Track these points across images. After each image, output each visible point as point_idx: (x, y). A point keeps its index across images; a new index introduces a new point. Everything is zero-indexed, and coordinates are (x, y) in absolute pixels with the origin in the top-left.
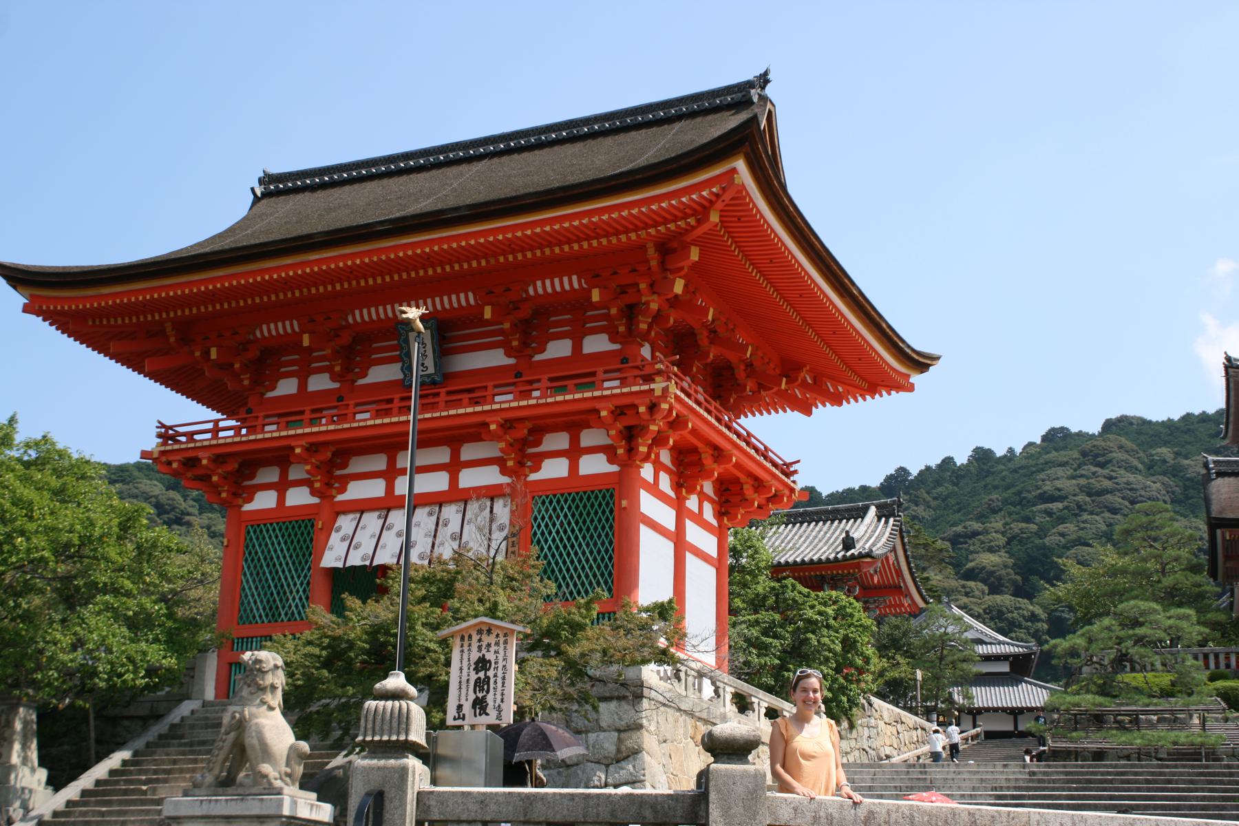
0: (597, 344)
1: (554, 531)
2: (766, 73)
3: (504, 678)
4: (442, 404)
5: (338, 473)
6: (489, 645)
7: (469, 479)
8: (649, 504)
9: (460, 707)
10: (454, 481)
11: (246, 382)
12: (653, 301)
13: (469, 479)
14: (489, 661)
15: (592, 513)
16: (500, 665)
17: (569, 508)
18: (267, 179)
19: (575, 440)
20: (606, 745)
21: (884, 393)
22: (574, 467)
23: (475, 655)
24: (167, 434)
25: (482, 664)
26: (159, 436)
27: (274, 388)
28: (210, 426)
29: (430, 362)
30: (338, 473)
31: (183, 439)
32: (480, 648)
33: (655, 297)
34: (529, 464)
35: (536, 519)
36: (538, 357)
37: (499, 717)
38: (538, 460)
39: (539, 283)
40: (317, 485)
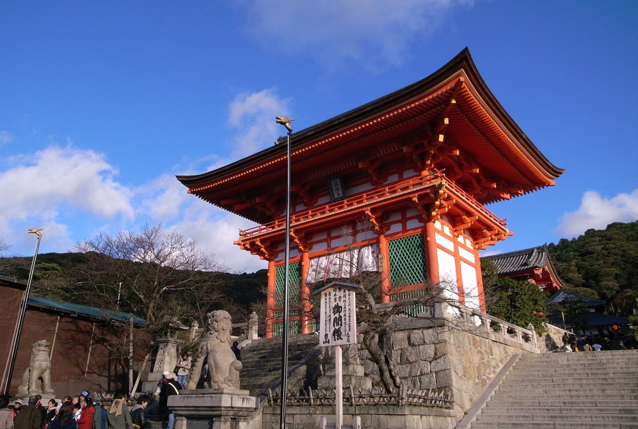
1: (399, 256)
3: (350, 316)
5: (309, 242)
6: (340, 297)
8: (439, 239)
9: (326, 335)
12: (431, 149)
14: (341, 307)
15: (413, 242)
16: (347, 309)
17: (404, 244)
19: (404, 215)
20: (429, 351)
21: (541, 188)
23: (333, 304)
24: (243, 234)
25: (337, 309)
26: (241, 235)
28: (258, 228)
29: (340, 192)
31: (249, 235)
33: (433, 148)
34: (385, 228)
35: (390, 251)
37: (348, 341)
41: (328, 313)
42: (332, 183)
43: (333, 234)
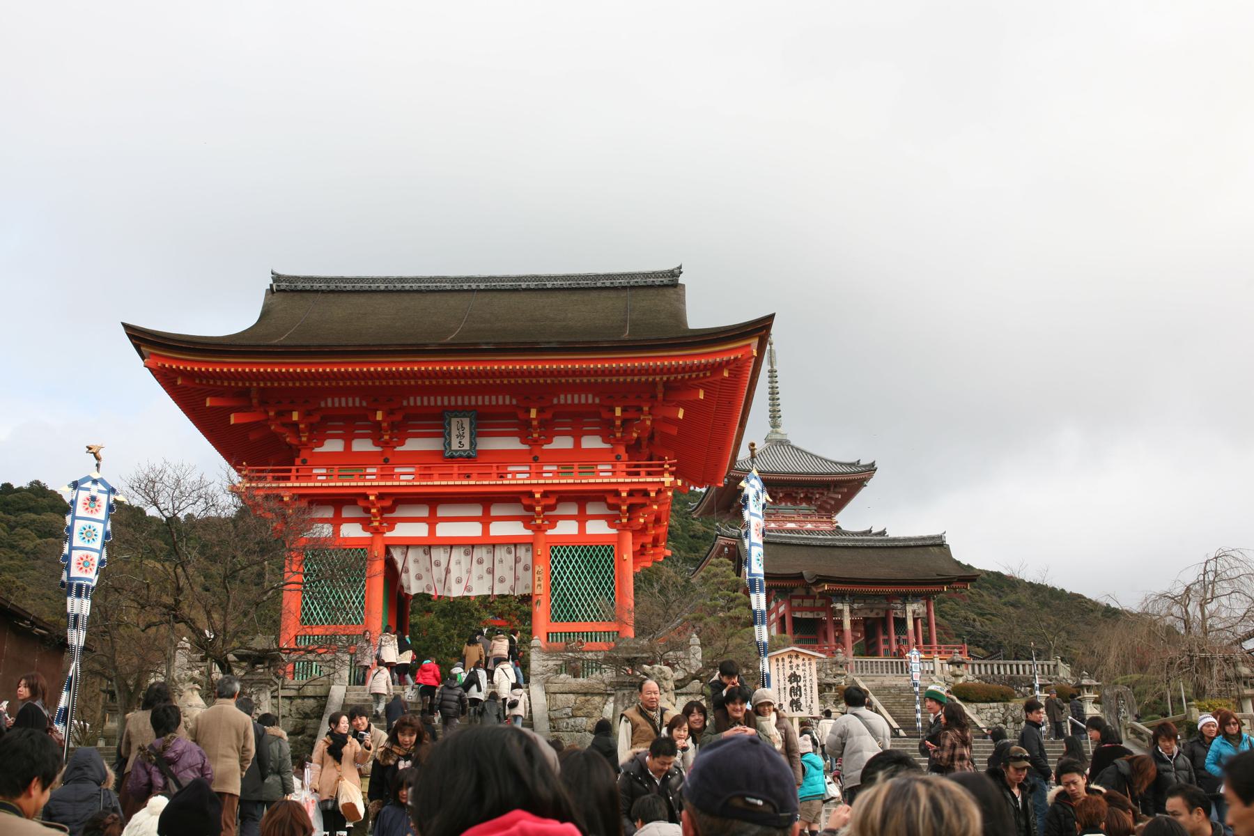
0: (592, 442)
2: (680, 267)
4: (495, 476)
7: (498, 529)
10: (486, 530)
11: (304, 439)
13: (498, 529)
18: (277, 278)
19: (582, 509)
22: (582, 528)
23: (788, 672)
25: (794, 678)
27: (321, 445)
30: (386, 515)
32: (791, 667)
36: (546, 447)
37: (811, 712)
38: (553, 522)
39: (562, 397)
40: (376, 524)
41: (782, 681)
42: (454, 421)
43: (442, 512)
